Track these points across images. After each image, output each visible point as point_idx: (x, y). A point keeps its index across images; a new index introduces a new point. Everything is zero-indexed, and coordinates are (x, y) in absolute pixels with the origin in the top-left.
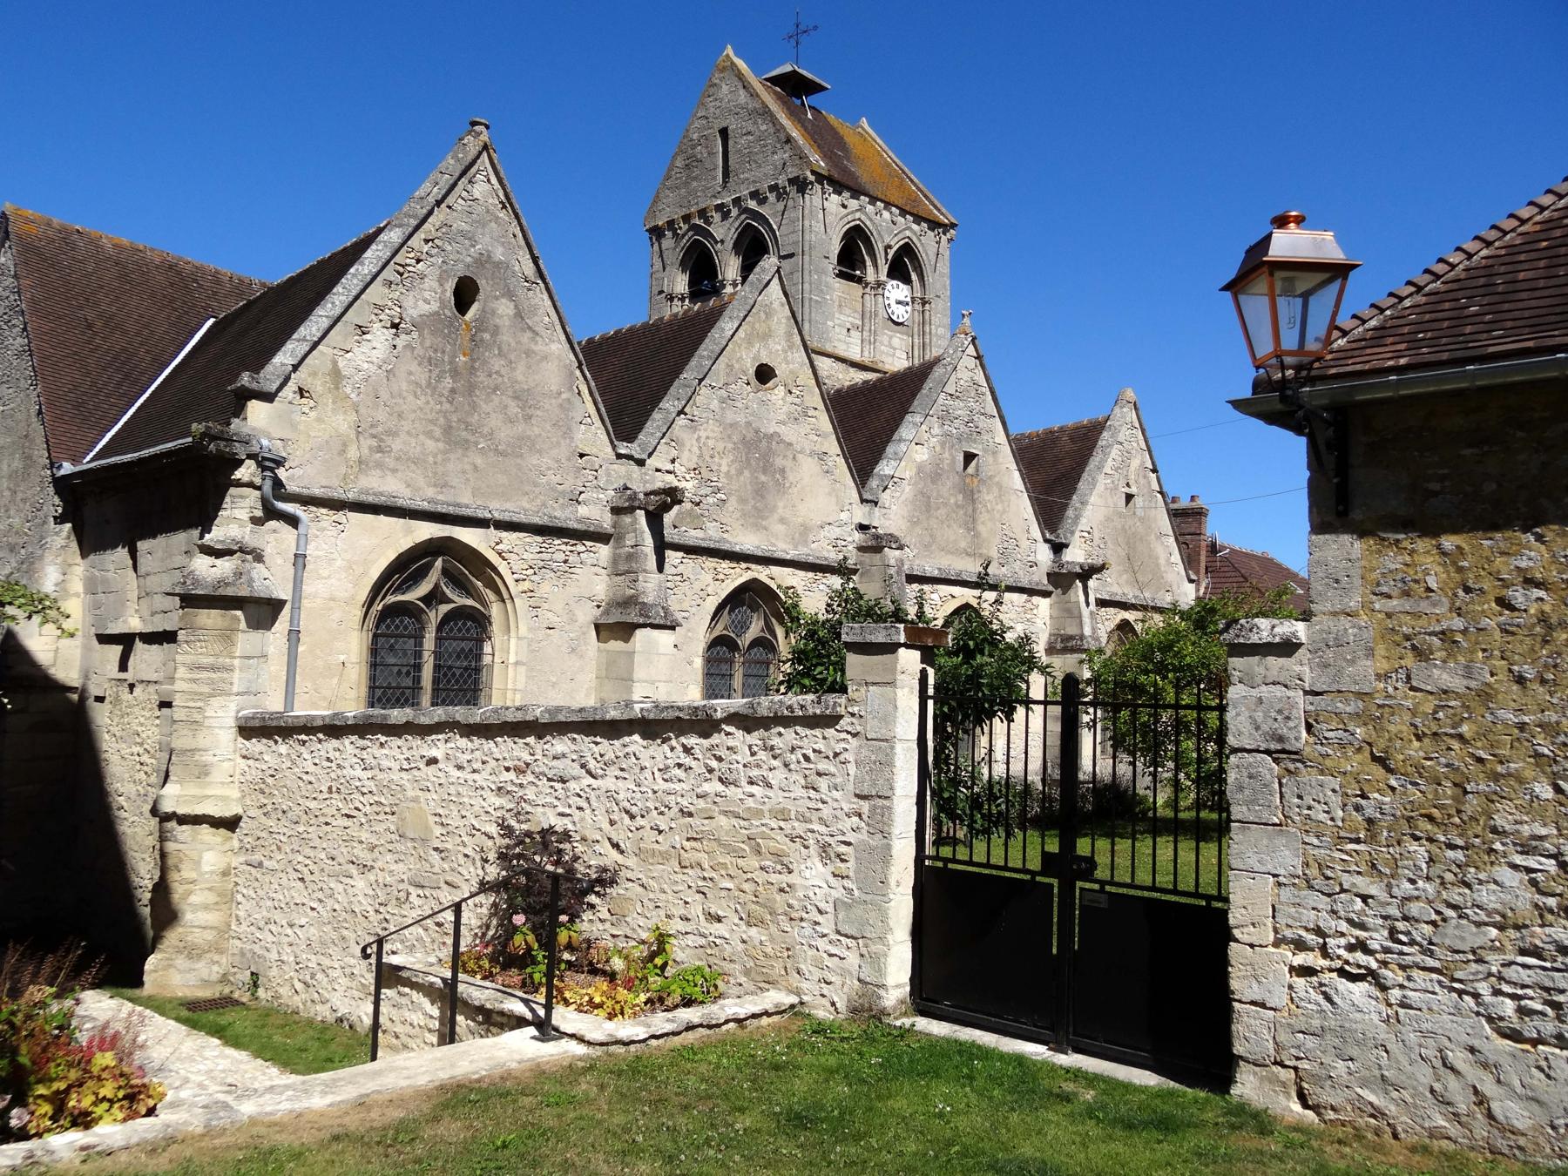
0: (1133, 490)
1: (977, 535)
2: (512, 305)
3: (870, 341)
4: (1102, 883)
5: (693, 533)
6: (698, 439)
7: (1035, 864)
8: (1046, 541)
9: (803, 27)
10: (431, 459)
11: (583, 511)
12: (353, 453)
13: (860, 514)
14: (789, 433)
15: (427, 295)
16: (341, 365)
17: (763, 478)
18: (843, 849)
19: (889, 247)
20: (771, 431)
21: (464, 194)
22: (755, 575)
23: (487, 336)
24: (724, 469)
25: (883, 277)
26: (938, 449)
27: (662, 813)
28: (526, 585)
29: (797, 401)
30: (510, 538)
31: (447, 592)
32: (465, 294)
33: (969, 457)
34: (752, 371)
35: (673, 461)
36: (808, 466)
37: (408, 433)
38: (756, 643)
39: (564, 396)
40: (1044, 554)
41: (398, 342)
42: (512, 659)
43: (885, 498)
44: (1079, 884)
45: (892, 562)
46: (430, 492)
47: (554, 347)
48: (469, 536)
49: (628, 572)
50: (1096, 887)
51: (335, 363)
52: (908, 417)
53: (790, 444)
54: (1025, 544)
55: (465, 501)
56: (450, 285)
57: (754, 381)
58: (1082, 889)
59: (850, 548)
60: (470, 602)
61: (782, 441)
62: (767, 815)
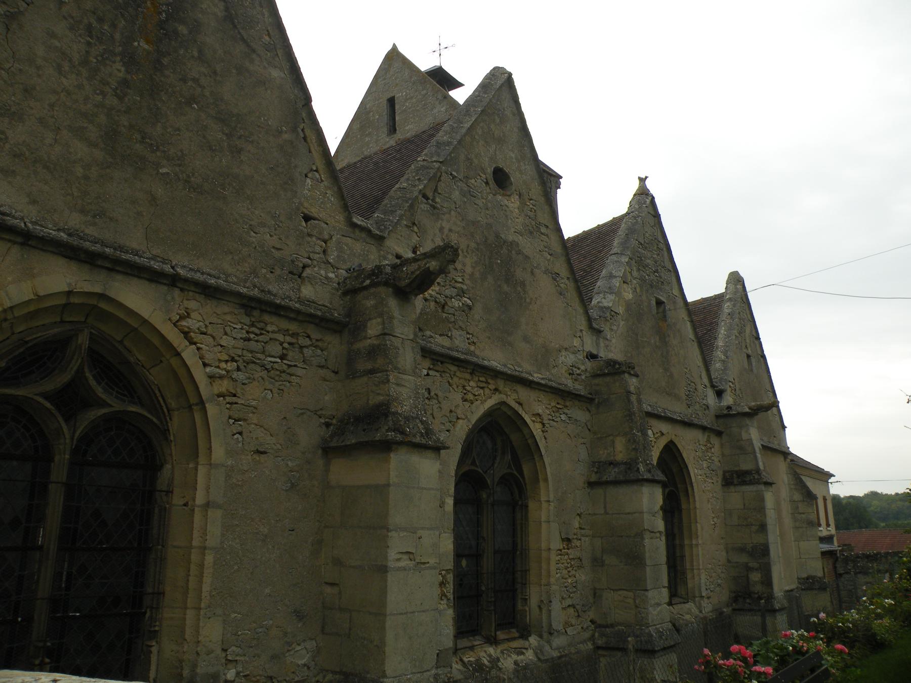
0: (750, 352)
1: (671, 376)
6: (441, 229)
9: (443, 46)
10: (79, 171)
11: (307, 291)
13: (589, 344)
17: (505, 288)
20: (510, 238)
22: (503, 397)
23: (183, 29)
26: (638, 290)
28: (224, 386)
29: (532, 214)
31: (99, 391)
33: (659, 303)
34: (490, 170)
36: (545, 282)
37: (41, 121)
38: (505, 480)
39: (286, 136)
40: (711, 399)
42: (200, 499)
45: (632, 389)
46: (75, 220)
47: (275, 73)
48: (136, 298)
49: (372, 372)
53: (527, 257)
54: (700, 387)
55: (134, 245)
59: (583, 377)
61: (519, 252)
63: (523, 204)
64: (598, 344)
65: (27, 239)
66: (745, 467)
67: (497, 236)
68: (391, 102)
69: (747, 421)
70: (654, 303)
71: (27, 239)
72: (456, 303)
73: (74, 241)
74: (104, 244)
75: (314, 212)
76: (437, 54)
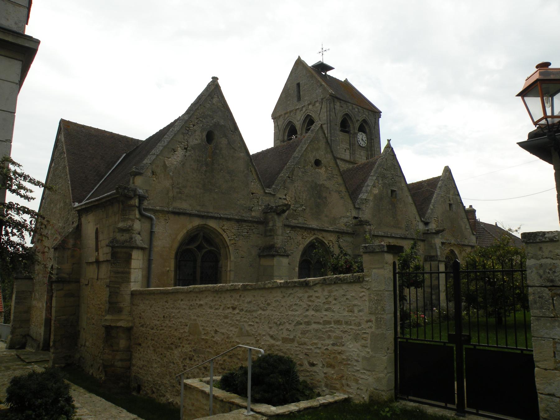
0: (452, 202)
2: (226, 140)
3: (353, 153)
4: (475, 346)
5: (294, 221)
6: (295, 187)
7: (445, 339)
8: (422, 221)
9: (324, 49)
11: (253, 214)
12: (171, 195)
13: (354, 214)
14: (327, 184)
15: (197, 137)
16: (167, 163)
17: (319, 200)
18: (365, 336)
19: (358, 120)
20: (321, 183)
21: (210, 102)
22: (317, 236)
23: (218, 151)
24: (304, 197)
25: (357, 131)
27: (290, 324)
28: (233, 242)
30: (227, 225)
32: (210, 137)
33: (393, 191)
34: (313, 162)
35: (286, 195)
40: (421, 227)
41: (187, 154)
42: (229, 269)
43: (363, 207)
44: (465, 346)
45: (367, 230)
46: (198, 208)
48: (212, 224)
49: (270, 236)
50: (472, 347)
51: (164, 162)
52: (370, 177)
53: (328, 188)
54: (414, 223)
56: (205, 134)
57: (314, 165)
58: (466, 348)
60: (213, 249)
62: (333, 323)
63: (327, 169)
64: (358, 213)
65: (191, 215)
66: (433, 254)
67: (316, 184)
68: (298, 85)
69: (435, 236)
70: (390, 192)
71: (191, 215)
72: (300, 209)
73: (199, 213)
74: (205, 212)
75: (254, 191)
76: (321, 54)
